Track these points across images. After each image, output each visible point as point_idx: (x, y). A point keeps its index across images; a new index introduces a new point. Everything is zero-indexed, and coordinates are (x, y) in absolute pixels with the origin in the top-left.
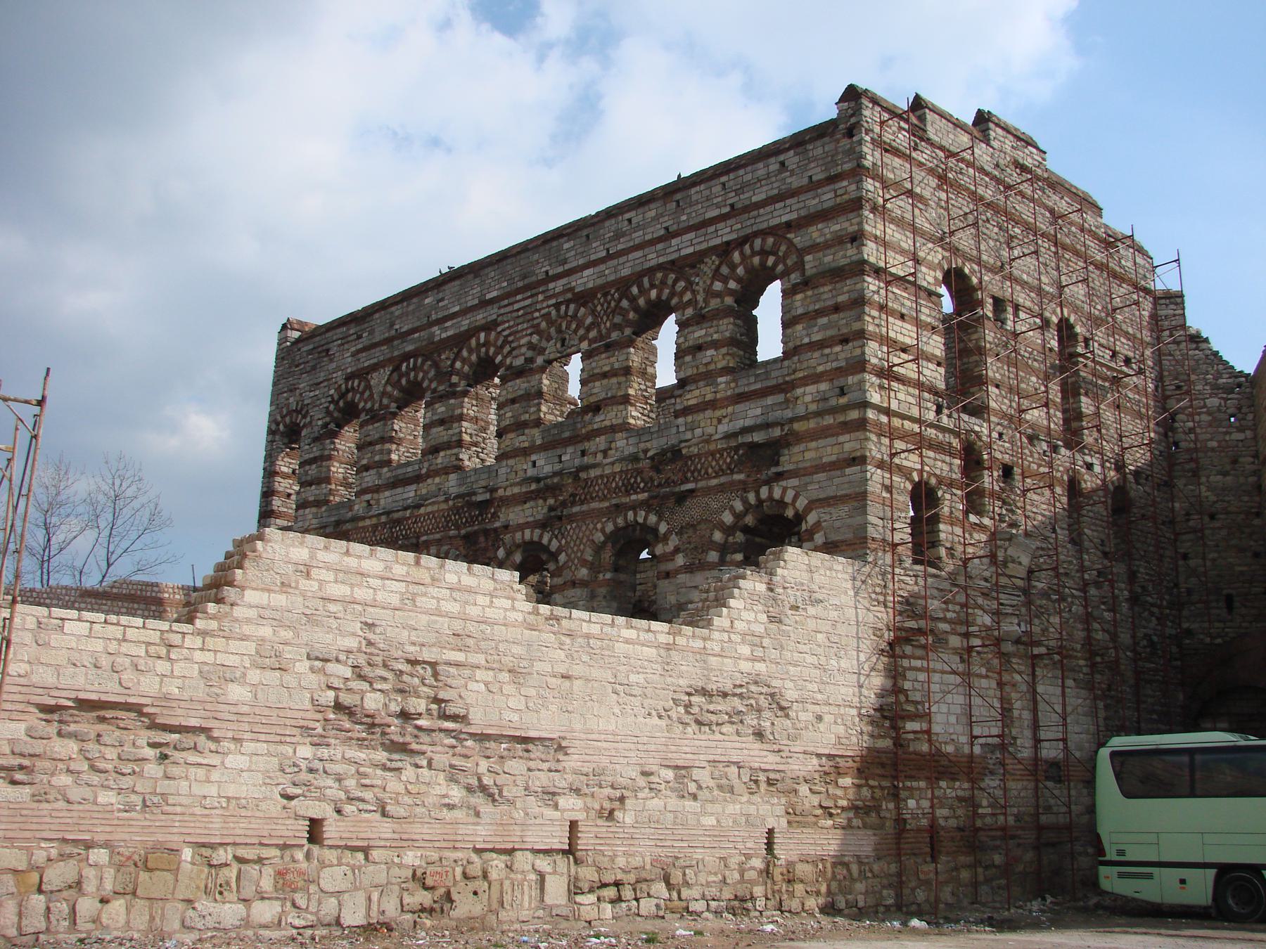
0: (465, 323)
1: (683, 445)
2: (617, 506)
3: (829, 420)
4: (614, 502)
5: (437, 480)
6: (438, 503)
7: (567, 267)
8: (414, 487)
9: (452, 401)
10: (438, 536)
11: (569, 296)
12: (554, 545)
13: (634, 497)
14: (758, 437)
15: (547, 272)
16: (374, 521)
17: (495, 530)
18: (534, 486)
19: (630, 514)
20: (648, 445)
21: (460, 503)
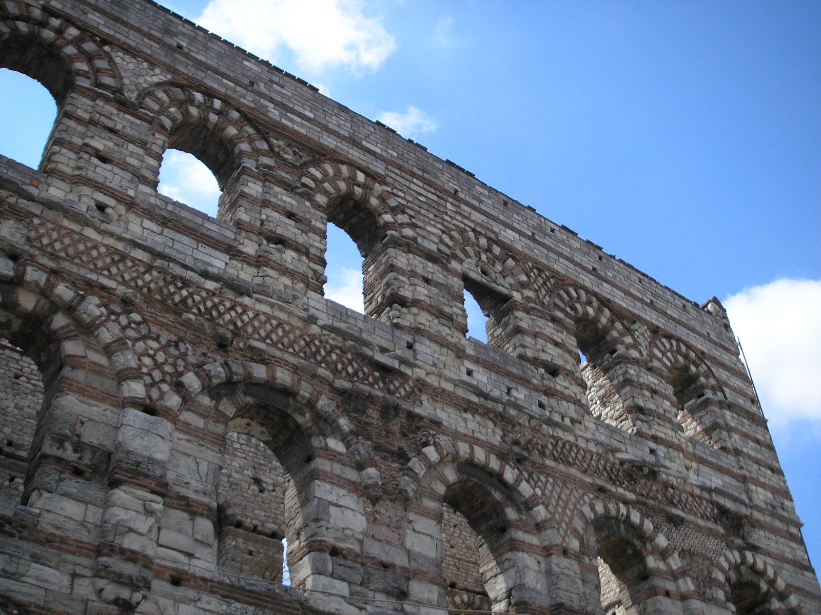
0: (329, 142)
1: (662, 469)
2: (602, 490)
3: (778, 524)
4: (600, 482)
5: (286, 281)
6: (290, 314)
7: (483, 207)
8: (226, 258)
9: (308, 204)
10: (292, 360)
11: (493, 236)
12: (525, 489)
13: (620, 490)
14: (729, 504)
15: (456, 191)
16: (120, 246)
17: (420, 418)
18: (474, 399)
19: (623, 509)
20: (623, 448)
21: (333, 340)
